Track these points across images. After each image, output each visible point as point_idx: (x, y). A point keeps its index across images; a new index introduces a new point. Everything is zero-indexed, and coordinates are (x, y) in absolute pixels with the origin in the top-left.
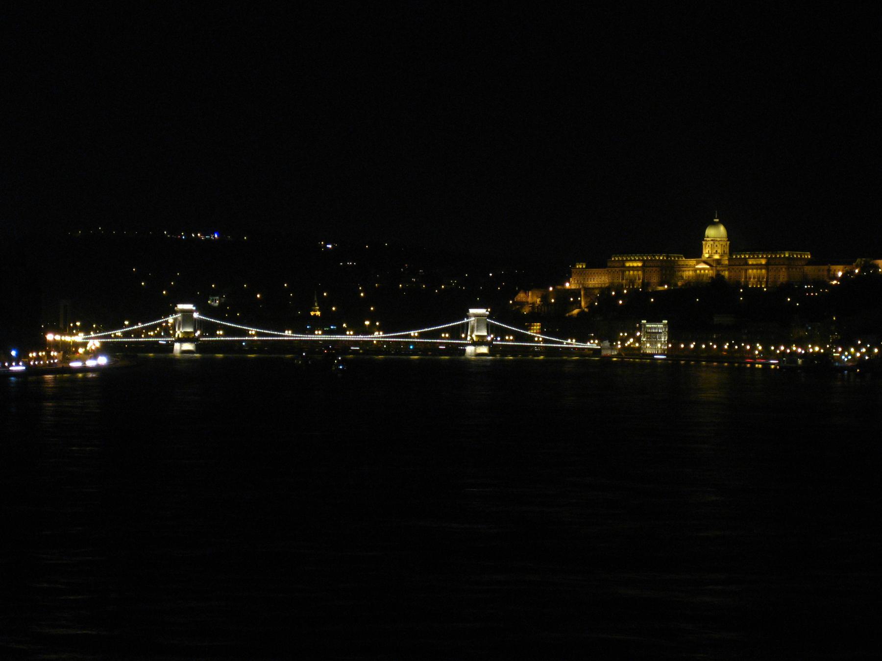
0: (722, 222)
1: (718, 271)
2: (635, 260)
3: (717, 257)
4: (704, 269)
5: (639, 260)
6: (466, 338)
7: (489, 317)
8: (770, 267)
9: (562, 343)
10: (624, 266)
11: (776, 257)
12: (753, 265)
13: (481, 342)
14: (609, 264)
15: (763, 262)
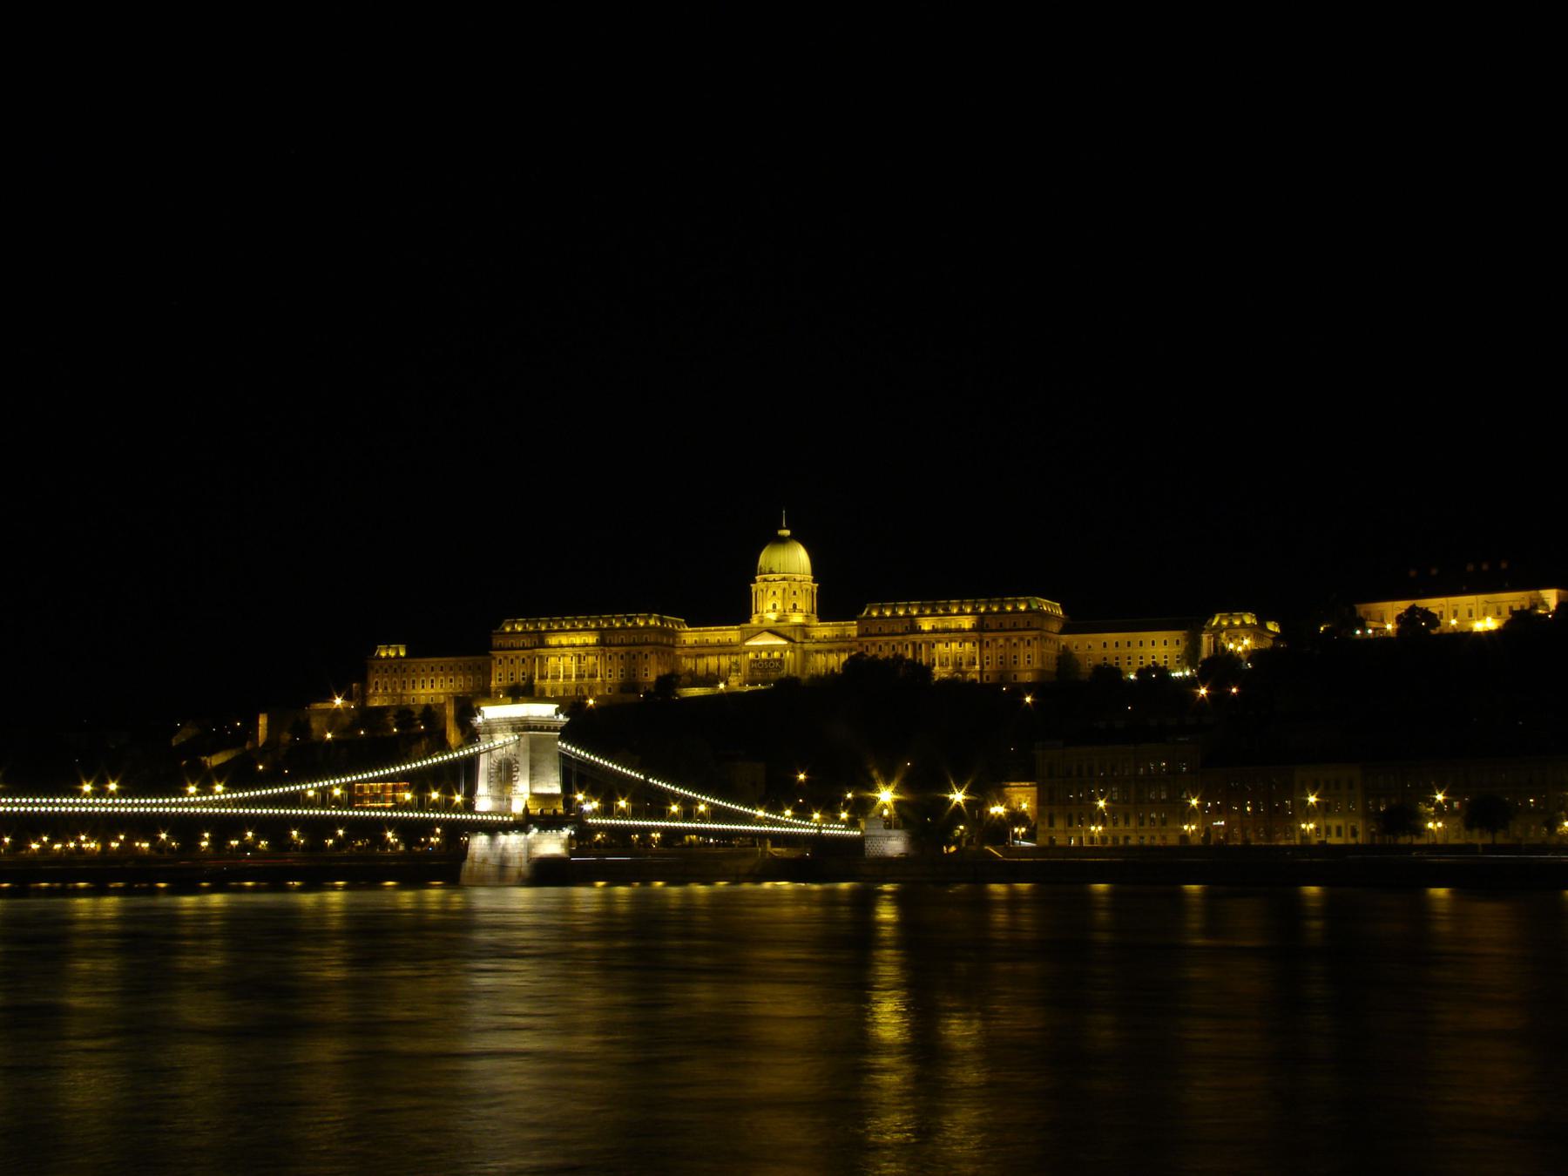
0: (798, 537)
1: (806, 654)
2: (574, 630)
3: (797, 618)
4: (771, 649)
5: (587, 629)
6: (469, 806)
7: (567, 733)
8: (988, 636)
9: (748, 819)
10: (544, 645)
11: (1002, 611)
12: (934, 631)
13: (548, 823)
14: (497, 642)
15: (967, 623)
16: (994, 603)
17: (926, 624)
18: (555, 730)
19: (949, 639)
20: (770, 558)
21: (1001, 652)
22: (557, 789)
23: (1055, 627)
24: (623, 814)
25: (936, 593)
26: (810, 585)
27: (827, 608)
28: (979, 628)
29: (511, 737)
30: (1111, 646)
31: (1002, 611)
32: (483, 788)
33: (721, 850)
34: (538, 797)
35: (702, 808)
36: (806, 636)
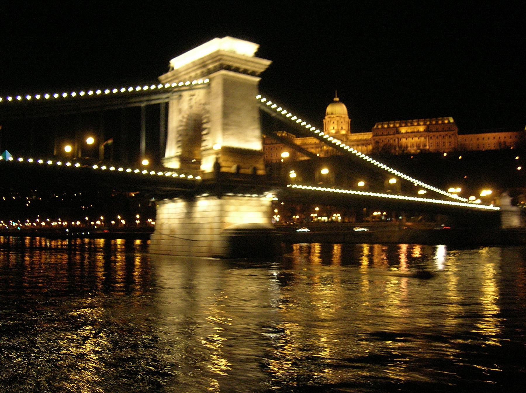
0: (342, 101)
3: (343, 132)
8: (431, 134)
12: (407, 133)
15: (422, 129)
17: (403, 130)
18: (253, 74)
20: (329, 109)
21: (437, 141)
24: (326, 182)
25: (407, 117)
26: (347, 119)
27: (355, 128)
28: (427, 130)
30: (481, 140)
35: (393, 181)
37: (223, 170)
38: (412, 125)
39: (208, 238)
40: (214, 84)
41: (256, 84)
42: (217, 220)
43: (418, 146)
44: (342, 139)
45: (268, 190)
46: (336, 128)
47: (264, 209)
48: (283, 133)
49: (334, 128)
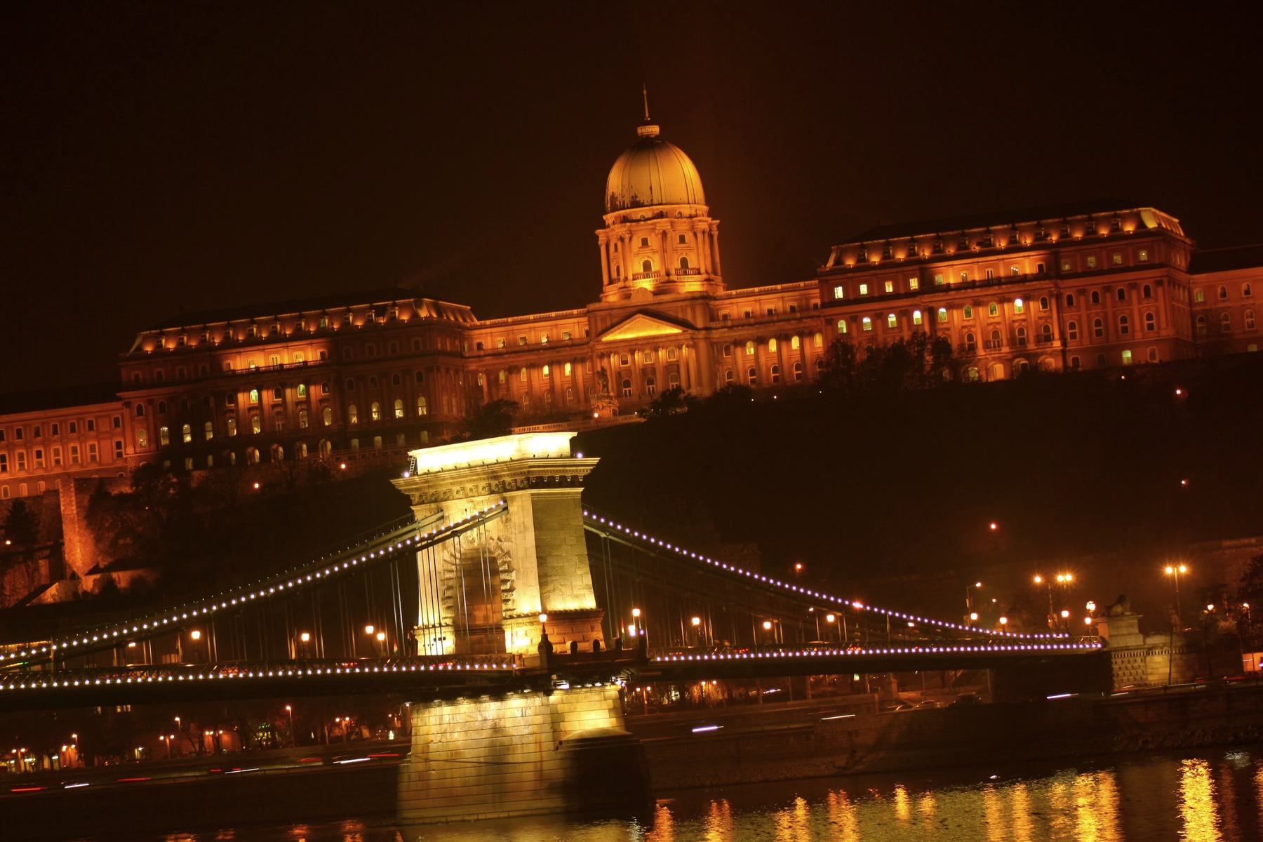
0: (676, 137)
2: (277, 339)
3: (692, 285)
4: (653, 344)
5: (300, 336)
8: (1069, 287)
11: (1091, 238)
13: (583, 669)
15: (1026, 265)
16: (1074, 225)
18: (574, 483)
19: (989, 304)
22: (589, 602)
23: (1181, 261)
26: (705, 223)
27: (744, 260)
29: (486, 503)
31: (1091, 238)
32: (431, 612)
33: (792, 705)
34: (560, 618)
36: (713, 317)
37: (557, 649)
38: (989, 250)
39: (534, 757)
40: (513, 508)
41: (579, 496)
42: (548, 728)
43: (1018, 342)
44: (689, 318)
45: (617, 673)
46: (655, 267)
47: (610, 703)
48: (419, 306)
49: (647, 266)
